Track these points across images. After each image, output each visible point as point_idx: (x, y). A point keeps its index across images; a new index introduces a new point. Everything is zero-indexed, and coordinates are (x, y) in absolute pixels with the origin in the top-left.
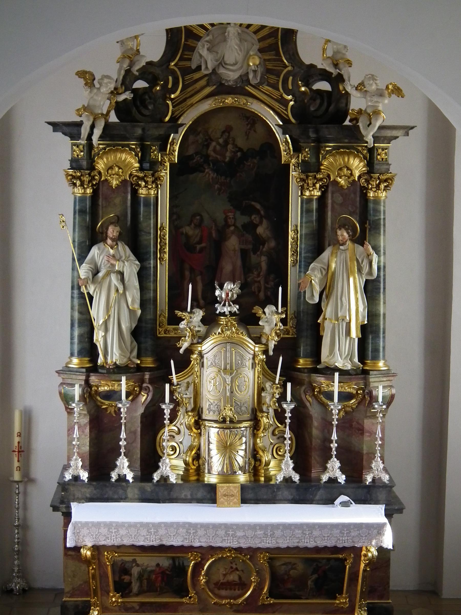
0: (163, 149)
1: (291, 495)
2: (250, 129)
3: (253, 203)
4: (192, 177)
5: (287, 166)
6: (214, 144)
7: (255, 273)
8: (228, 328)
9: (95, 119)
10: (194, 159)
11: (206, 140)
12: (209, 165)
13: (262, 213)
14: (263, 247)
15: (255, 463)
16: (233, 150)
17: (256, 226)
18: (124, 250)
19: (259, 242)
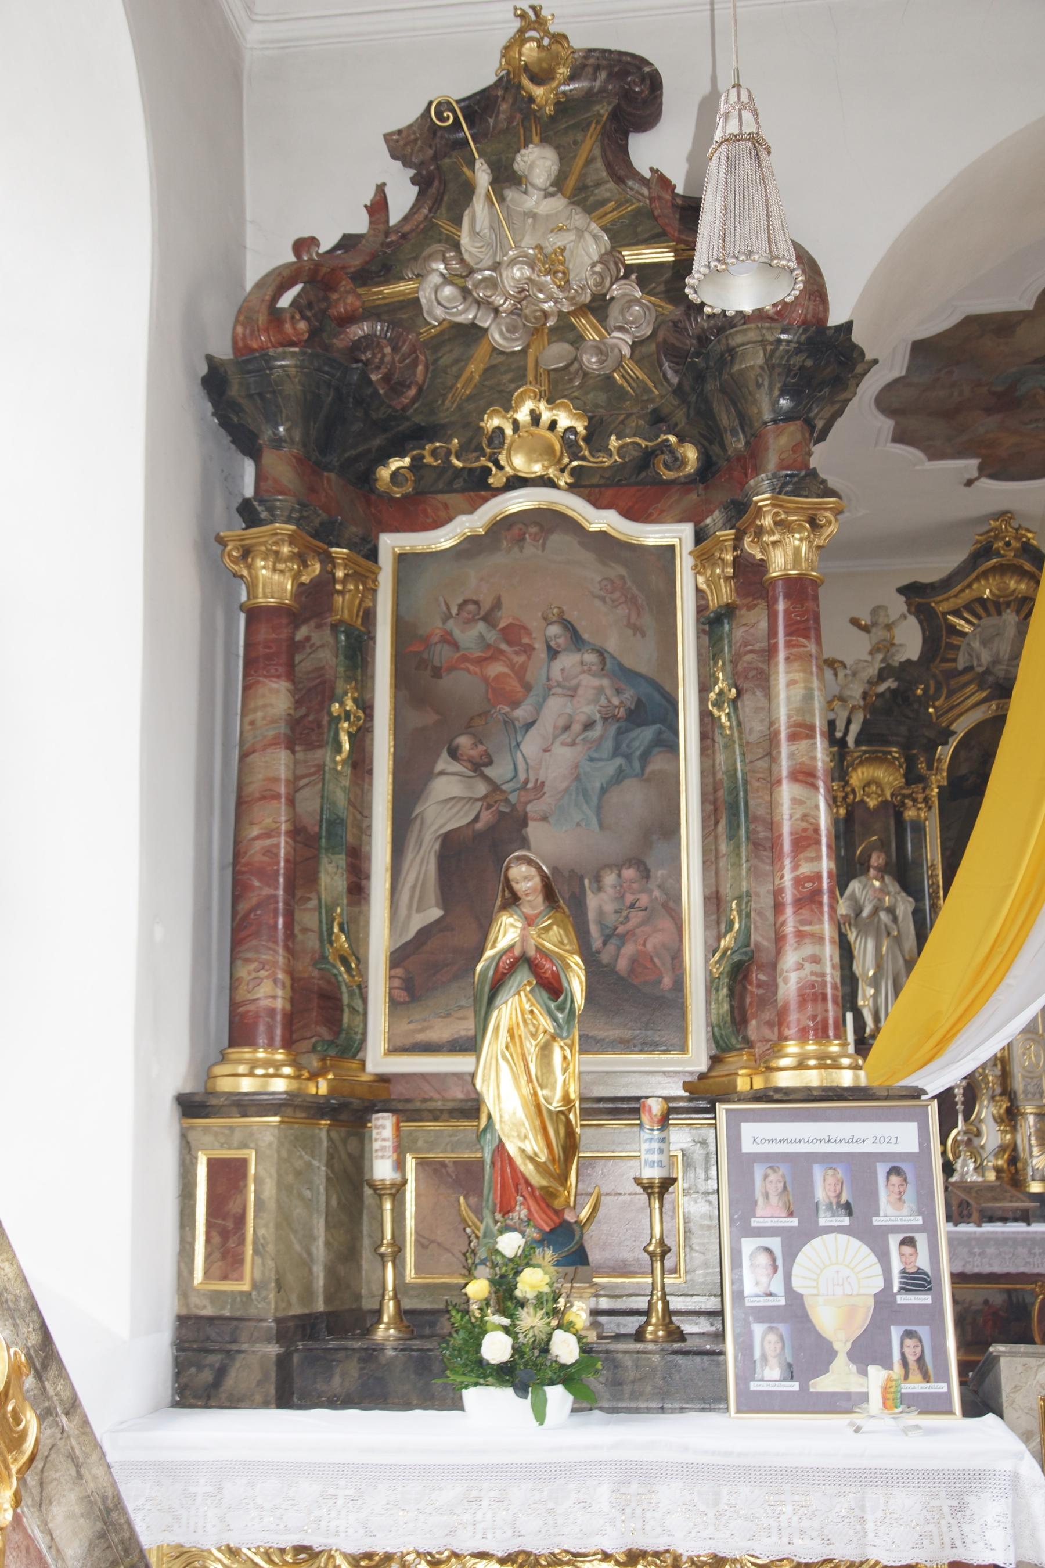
0: (930, 767)
9: (851, 713)
18: (893, 887)
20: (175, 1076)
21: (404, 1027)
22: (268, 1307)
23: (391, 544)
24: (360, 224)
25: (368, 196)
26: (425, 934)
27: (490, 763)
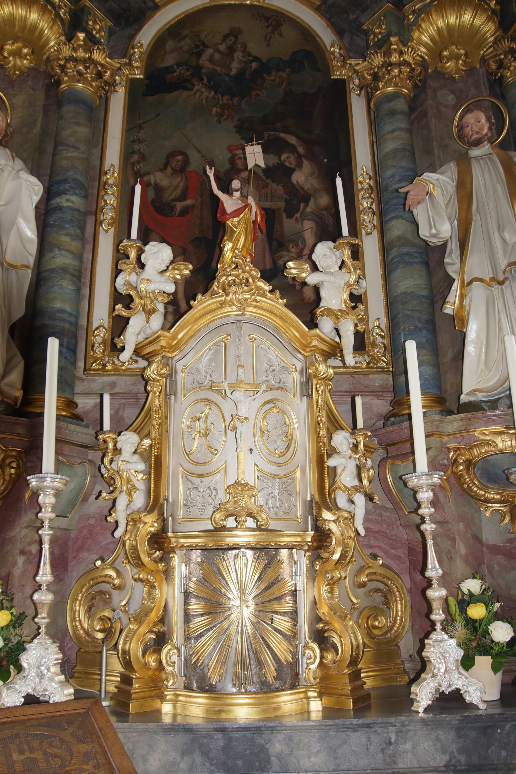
1: (444, 751)
2: (272, 32)
3: (282, 135)
4: (169, 97)
5: (341, 86)
6: (210, 51)
7: (293, 250)
10: (174, 72)
11: (197, 47)
12: (201, 79)
13: (301, 150)
14: (306, 206)
15: (322, 657)
16: (244, 59)
17: (291, 171)
19: (297, 198)
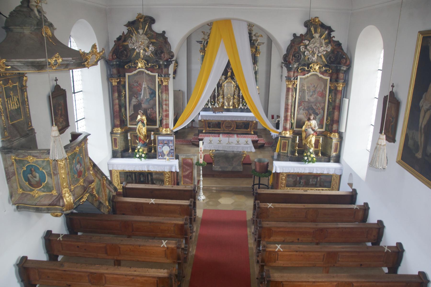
8: (229, 80)
20: (110, 131)
21: (131, 123)
22: (120, 150)
23: (127, 74)
24: (122, 35)
25: (122, 32)
26: (132, 114)
27: (138, 98)
